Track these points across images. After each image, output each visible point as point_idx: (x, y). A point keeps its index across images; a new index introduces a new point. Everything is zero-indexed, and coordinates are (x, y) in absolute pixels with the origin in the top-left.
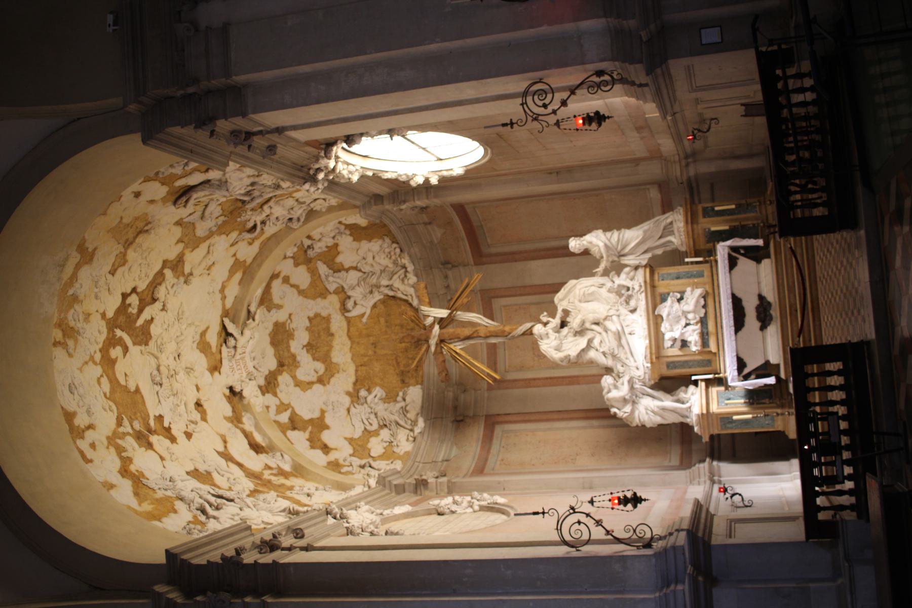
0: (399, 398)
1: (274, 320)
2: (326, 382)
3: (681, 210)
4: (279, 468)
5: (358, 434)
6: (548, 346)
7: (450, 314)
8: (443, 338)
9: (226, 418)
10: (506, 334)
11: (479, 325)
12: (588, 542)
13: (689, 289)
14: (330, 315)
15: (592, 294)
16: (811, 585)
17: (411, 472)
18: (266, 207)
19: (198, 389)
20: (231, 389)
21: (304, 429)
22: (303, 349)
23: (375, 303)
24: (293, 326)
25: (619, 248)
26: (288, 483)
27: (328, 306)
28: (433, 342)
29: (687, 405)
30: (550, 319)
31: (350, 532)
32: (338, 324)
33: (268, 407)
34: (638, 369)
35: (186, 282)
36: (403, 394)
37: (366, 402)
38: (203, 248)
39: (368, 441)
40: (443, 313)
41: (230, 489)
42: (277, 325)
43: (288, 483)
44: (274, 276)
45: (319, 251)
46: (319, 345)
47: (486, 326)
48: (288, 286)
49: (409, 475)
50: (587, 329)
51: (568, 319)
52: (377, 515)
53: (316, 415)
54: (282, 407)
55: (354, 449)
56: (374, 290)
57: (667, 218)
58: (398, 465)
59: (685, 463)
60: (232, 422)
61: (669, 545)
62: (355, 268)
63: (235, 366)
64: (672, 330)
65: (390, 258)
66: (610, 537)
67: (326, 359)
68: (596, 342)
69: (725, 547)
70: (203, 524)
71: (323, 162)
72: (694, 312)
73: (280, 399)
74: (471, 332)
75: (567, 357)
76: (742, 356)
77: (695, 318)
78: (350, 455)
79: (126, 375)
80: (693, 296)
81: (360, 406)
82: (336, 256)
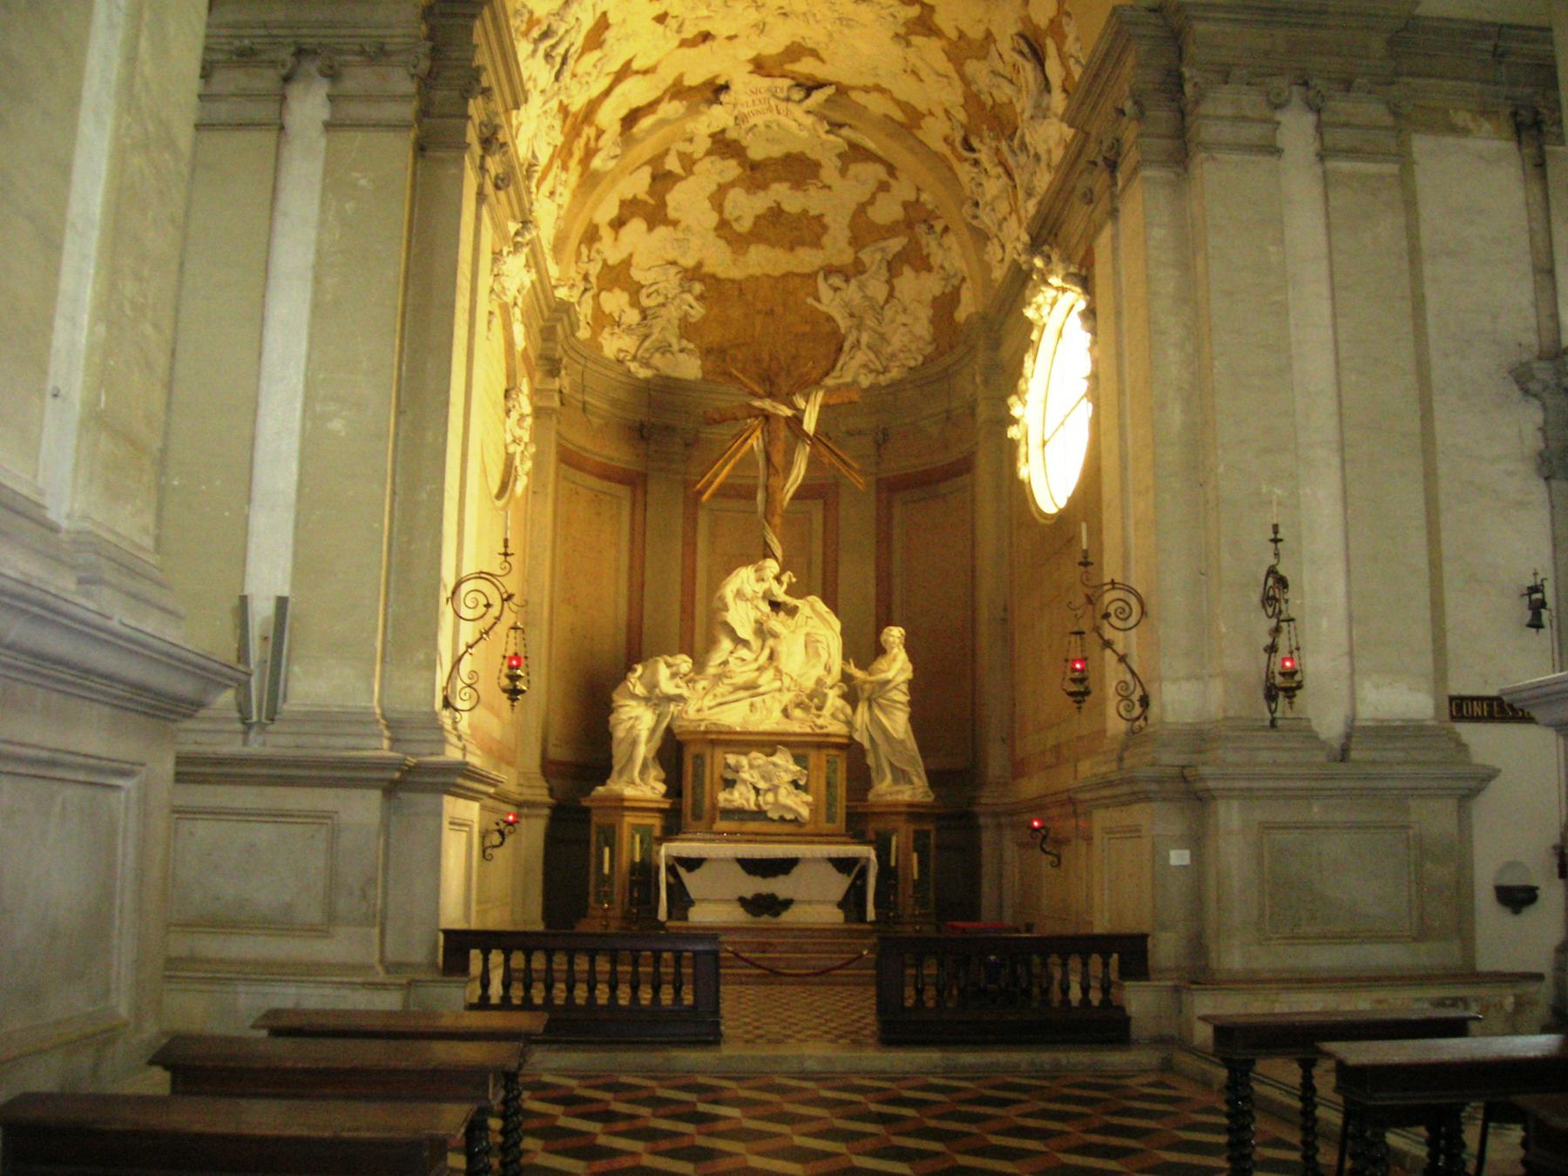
0: (684, 343)
3: (930, 798)
4: (597, 150)
5: (637, 274)
7: (807, 435)
9: (681, 76)
10: (769, 517)
11: (786, 478)
12: (457, 615)
13: (809, 798)
15: (817, 654)
16: (377, 930)
17: (573, 354)
18: (1000, 170)
19: (730, 38)
20: (725, 88)
21: (652, 192)
23: (834, 320)
24: (813, 191)
26: (573, 163)
27: (837, 247)
28: (767, 404)
29: (637, 780)
31: (497, 256)
32: (807, 259)
33: (691, 140)
34: (699, 710)
35: (897, 35)
37: (683, 292)
38: (949, 68)
39: (623, 289)
40: (809, 425)
41: (574, 75)
43: (573, 163)
44: (891, 170)
45: (924, 242)
50: (764, 641)
51: (782, 614)
52: (516, 298)
53: (672, 213)
54: (688, 162)
57: (919, 777)
58: (584, 333)
59: (548, 767)
60: (674, 85)
61: (446, 734)
62: (891, 295)
63: (760, 96)
64: (751, 766)
66: (462, 649)
67: (757, 235)
68: (743, 652)
69: (438, 813)
70: (526, 34)
71: (1060, 268)
72: (777, 804)
73: (700, 159)
75: (726, 608)
76: (705, 867)
77: (767, 803)
80: (799, 804)
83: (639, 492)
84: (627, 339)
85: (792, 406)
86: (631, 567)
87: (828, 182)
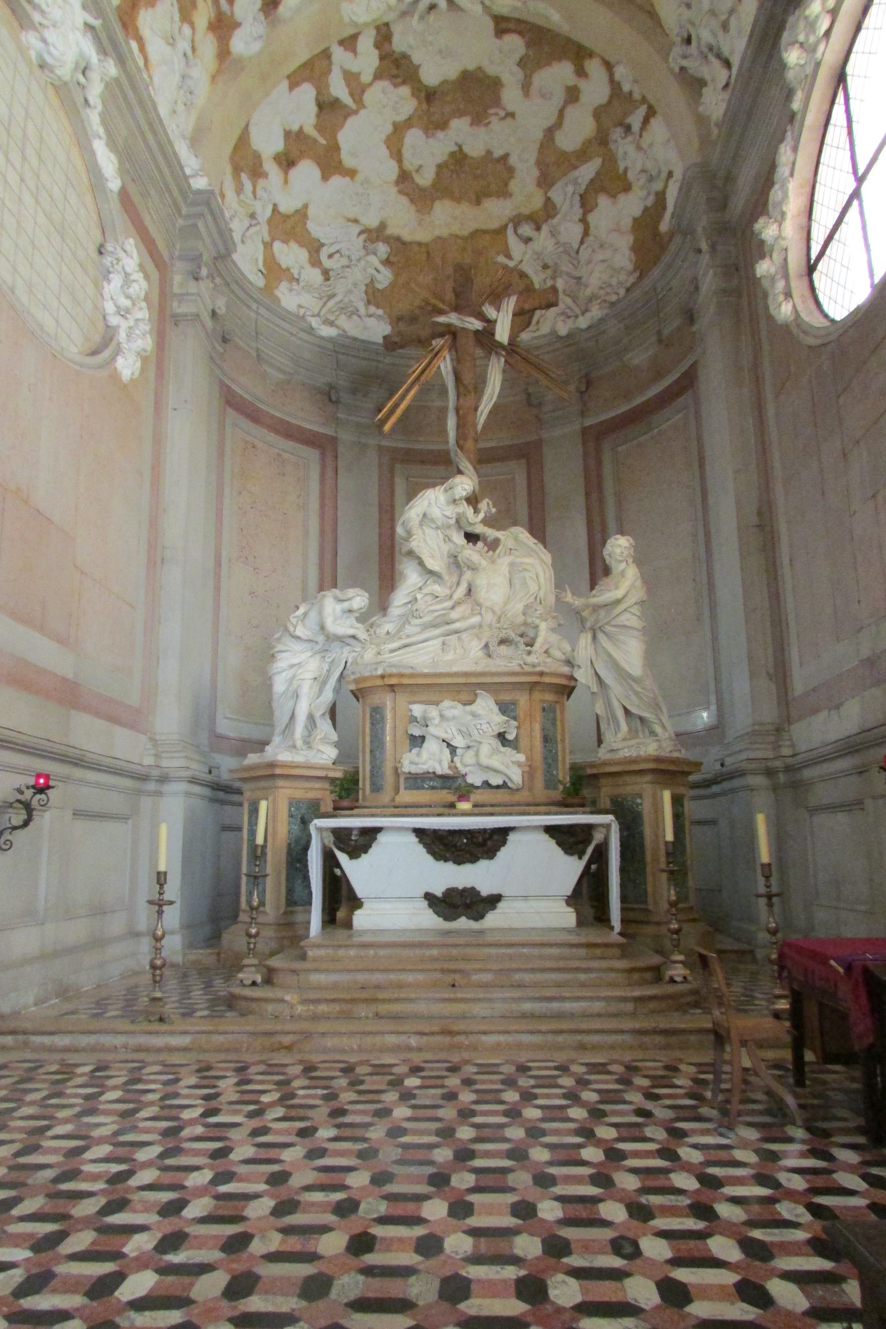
0: (372, 309)
1: (506, 78)
2: (401, 186)
5: (315, 229)
6: (433, 501)
7: (501, 345)
8: (459, 335)
11: (479, 399)
13: (521, 758)
21: (319, 127)
22: (456, 144)
23: (526, 276)
24: (496, 125)
25: (608, 628)
28: (452, 319)
29: (299, 743)
30: (481, 515)
36: (379, 316)
37: (368, 254)
39: (302, 245)
46: (463, 176)
47: (476, 409)
48: (562, 103)
49: (229, 281)
50: (460, 576)
51: (480, 544)
53: (348, 161)
55: (288, 216)
56: (549, 272)
62: (586, 233)
65: (601, 288)
74: (466, 382)
77: (466, 766)
78: (275, 205)
81: (362, 245)
83: (329, 460)
85: (481, 316)
86: (322, 532)
87: (510, 108)
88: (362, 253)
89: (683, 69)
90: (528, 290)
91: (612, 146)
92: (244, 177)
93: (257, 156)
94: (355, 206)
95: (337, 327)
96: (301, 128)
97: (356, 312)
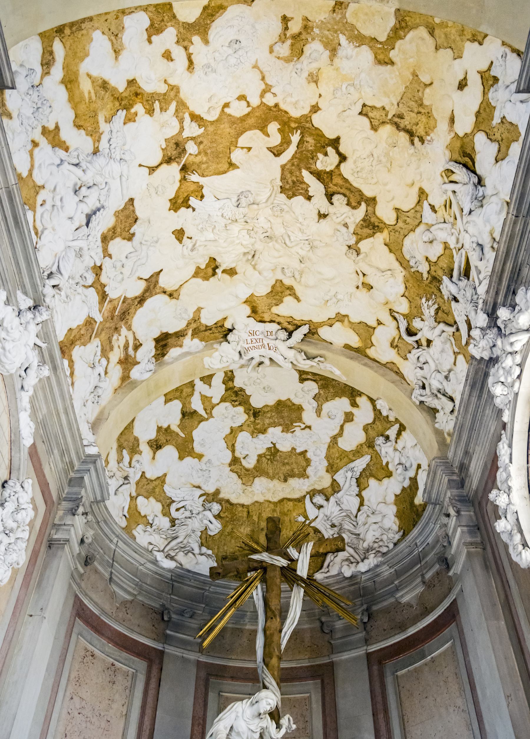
0: (204, 550)
2: (233, 467)
5: (169, 490)
6: (240, 714)
7: (302, 579)
14: (308, 477)
21: (182, 426)
23: (320, 532)
28: (265, 557)
30: (283, 731)
36: (209, 555)
37: (205, 510)
39: (158, 501)
42: (300, 409)
46: (275, 463)
47: (281, 631)
48: (342, 422)
53: (197, 448)
55: (152, 481)
56: (336, 529)
62: (362, 504)
63: (256, 337)
65: (375, 542)
73: (218, 404)
79: (249, 149)
81: (202, 503)
82: (376, 478)
84: (157, 536)
87: (308, 424)
88: (201, 509)
89: (422, 402)
90: (321, 540)
91: (377, 448)
92: (125, 452)
93: (137, 440)
94: (199, 477)
95: (176, 561)
96: (169, 426)
97: (191, 551)
